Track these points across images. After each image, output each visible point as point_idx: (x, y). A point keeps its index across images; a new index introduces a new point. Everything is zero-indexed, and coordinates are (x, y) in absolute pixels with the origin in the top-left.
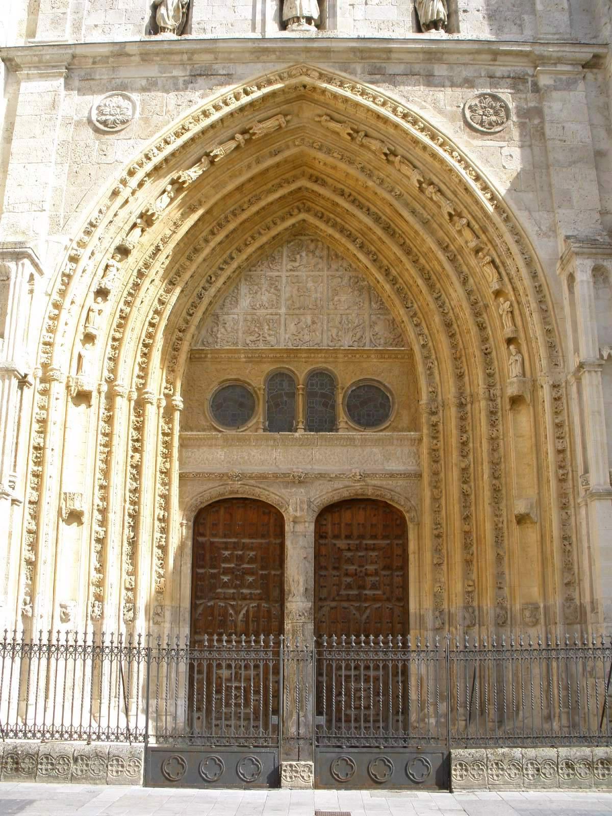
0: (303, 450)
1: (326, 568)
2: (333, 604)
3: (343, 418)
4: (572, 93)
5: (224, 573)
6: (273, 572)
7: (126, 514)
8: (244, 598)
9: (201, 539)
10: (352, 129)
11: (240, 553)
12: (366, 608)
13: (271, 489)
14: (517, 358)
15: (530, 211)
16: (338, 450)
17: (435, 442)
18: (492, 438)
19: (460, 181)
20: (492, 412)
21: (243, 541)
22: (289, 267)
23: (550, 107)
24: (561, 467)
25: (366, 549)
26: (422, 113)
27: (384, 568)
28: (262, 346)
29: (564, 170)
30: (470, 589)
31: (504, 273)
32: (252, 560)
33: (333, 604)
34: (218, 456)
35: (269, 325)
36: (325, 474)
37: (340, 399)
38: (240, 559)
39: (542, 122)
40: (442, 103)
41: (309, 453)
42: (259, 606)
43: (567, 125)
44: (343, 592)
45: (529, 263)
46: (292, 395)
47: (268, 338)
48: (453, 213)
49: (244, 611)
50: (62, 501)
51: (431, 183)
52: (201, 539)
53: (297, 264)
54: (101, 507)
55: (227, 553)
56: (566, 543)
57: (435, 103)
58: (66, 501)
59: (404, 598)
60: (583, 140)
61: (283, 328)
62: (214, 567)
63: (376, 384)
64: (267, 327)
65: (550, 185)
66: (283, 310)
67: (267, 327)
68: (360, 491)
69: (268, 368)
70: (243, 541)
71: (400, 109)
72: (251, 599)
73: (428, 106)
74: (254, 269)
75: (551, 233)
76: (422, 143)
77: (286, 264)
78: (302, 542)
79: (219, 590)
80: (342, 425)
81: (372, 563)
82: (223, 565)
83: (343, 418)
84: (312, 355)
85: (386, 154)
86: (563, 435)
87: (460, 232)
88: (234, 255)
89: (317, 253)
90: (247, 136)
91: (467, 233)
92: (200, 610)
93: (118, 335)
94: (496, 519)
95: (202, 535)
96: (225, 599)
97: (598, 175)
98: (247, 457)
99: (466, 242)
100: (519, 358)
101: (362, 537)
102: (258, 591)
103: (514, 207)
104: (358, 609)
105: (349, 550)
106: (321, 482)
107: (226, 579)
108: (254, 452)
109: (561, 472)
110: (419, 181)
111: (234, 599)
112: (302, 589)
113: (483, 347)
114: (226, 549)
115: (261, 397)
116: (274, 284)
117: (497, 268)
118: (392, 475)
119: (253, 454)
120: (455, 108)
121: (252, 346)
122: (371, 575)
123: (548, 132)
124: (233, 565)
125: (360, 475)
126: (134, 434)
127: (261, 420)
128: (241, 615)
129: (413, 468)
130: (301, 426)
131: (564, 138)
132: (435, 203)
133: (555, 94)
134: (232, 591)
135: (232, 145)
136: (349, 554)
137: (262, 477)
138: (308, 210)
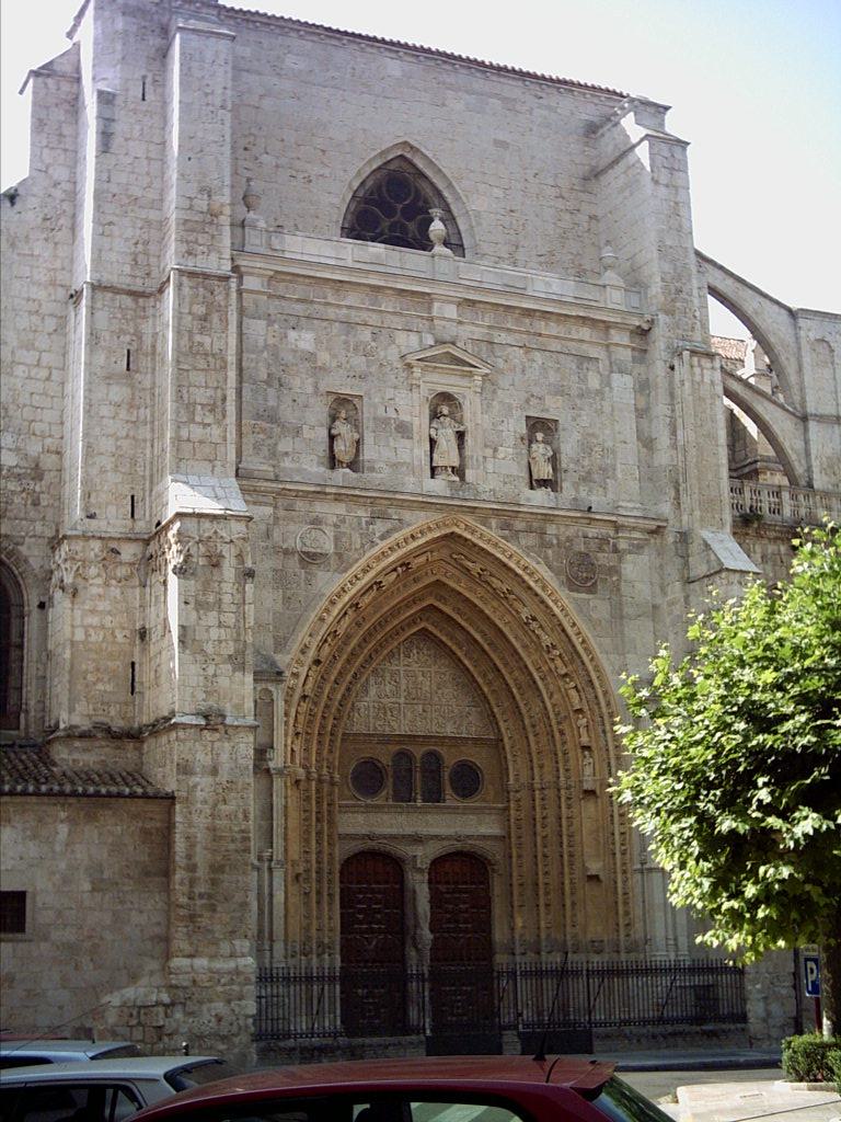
3: (448, 791)
26: (537, 566)
37: (446, 775)
44: (444, 926)
51: (534, 619)
71: (522, 562)
79: (356, 926)
83: (448, 791)
91: (558, 662)
100: (591, 760)
101: (456, 883)
107: (361, 916)
108: (385, 817)
117: (578, 691)
118: (484, 837)
136: (448, 896)
137: (393, 837)
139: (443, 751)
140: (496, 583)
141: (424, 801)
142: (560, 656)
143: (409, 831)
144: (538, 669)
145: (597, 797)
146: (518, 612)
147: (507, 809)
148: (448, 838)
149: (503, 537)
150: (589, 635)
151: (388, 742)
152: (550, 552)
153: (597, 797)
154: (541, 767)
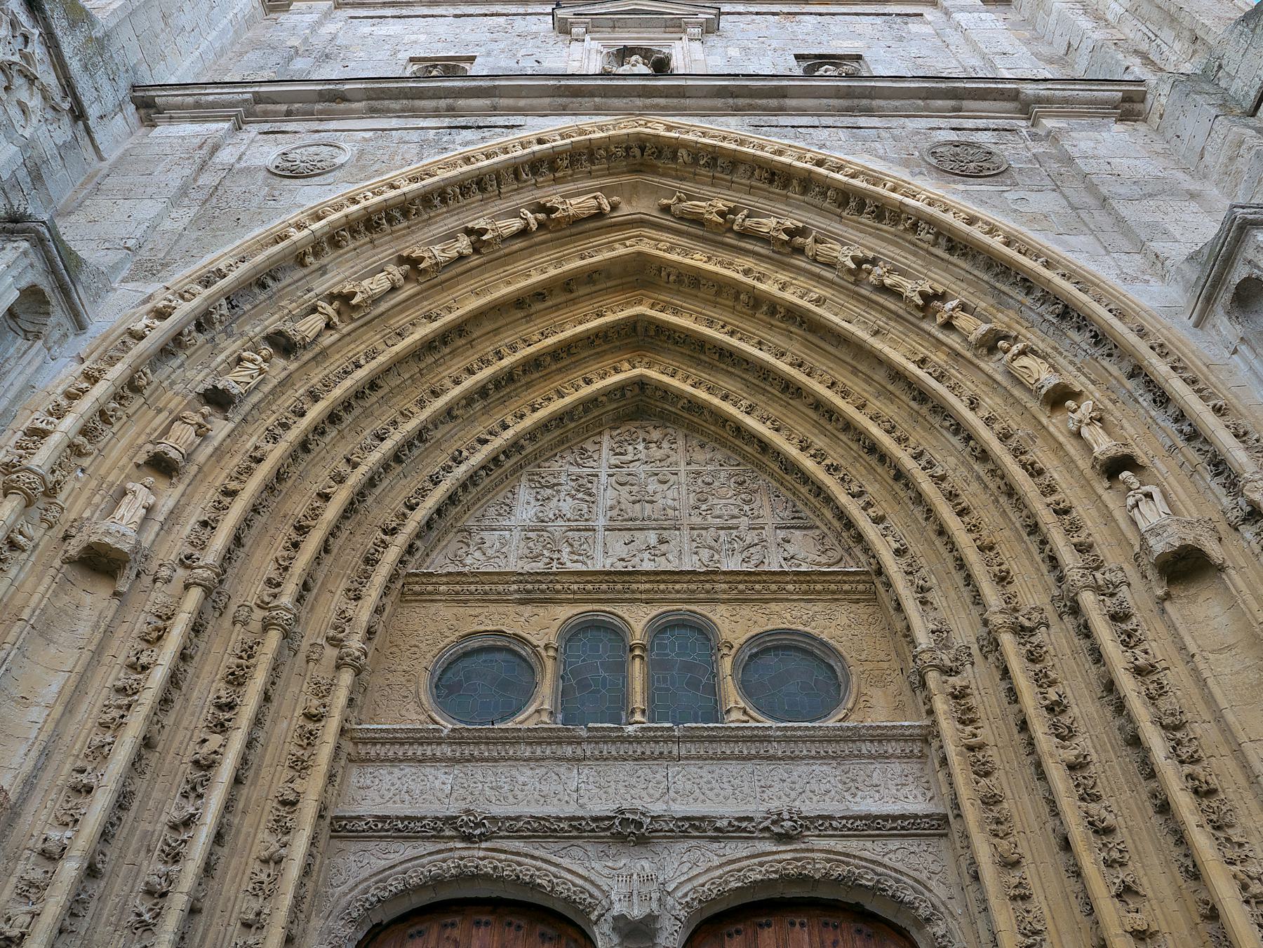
0: (644, 771)
13: (565, 862)
16: (733, 767)
17: (969, 729)
34: (437, 783)
35: (571, 545)
36: (702, 819)
41: (659, 776)
61: (600, 547)
64: (569, 549)
66: (601, 522)
67: (569, 549)
74: (547, 464)
90: (541, 216)
91: (963, 321)
98: (507, 787)
106: (693, 843)
115: (549, 664)
116: (585, 489)
119: (521, 779)
125: (791, 819)
126: (223, 693)
135: (516, 224)
140: (768, 225)
144: (922, 362)
145: (1221, 569)
146: (830, 265)
147: (929, 735)
153: (1221, 569)
154: (1003, 579)
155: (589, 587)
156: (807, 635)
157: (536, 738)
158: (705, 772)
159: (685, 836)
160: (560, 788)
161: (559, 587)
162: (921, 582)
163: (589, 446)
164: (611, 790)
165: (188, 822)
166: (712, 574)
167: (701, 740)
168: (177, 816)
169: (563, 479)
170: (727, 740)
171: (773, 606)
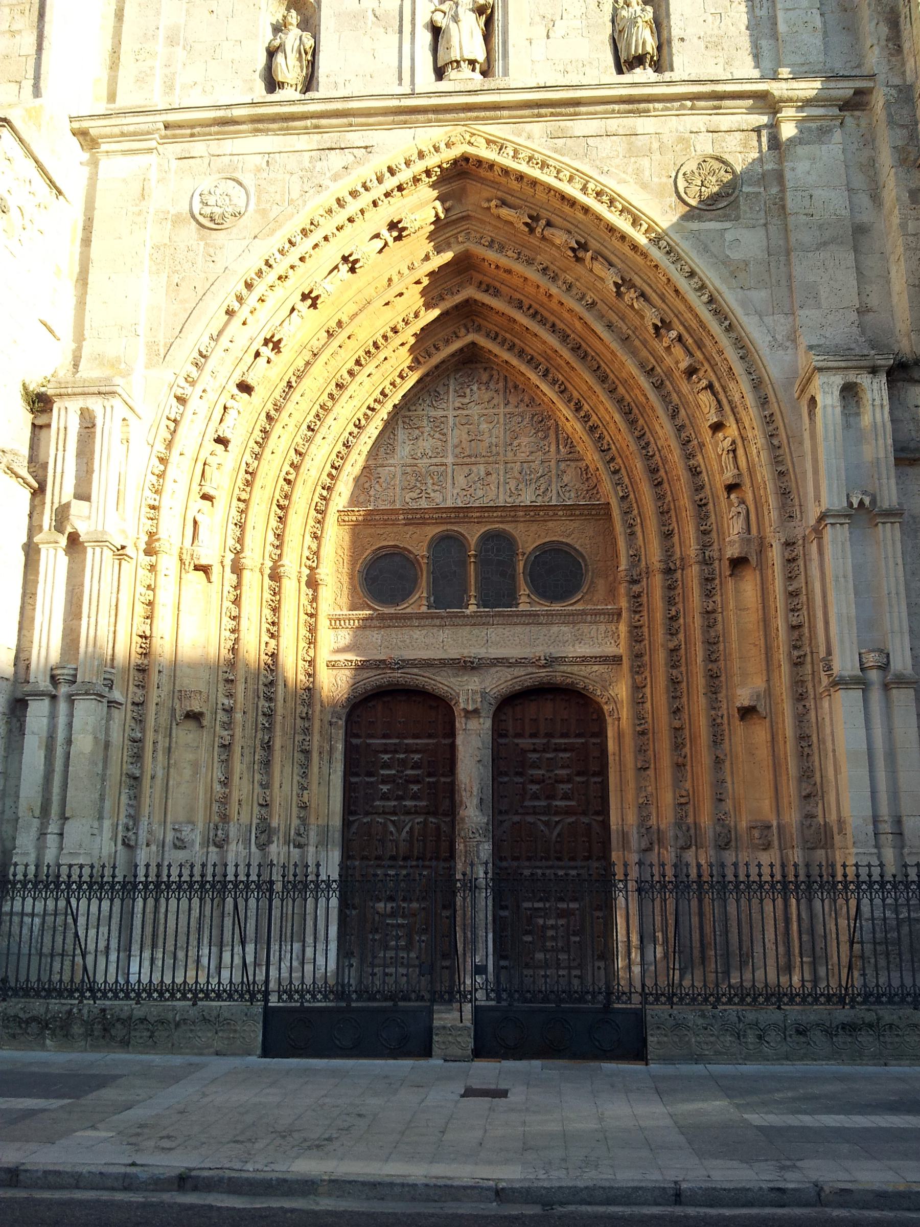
0: (476, 631)
1: (506, 774)
2: (516, 818)
3: (524, 590)
4: (824, 147)
5: (384, 782)
6: (443, 779)
7: (260, 713)
8: (408, 813)
9: (355, 741)
10: (530, 217)
11: (402, 756)
12: (557, 823)
13: (438, 678)
14: (739, 509)
15: (760, 316)
16: (519, 629)
17: (637, 617)
18: (708, 612)
19: (669, 280)
20: (707, 579)
21: (406, 741)
22: (457, 405)
23: (793, 169)
24: (795, 647)
25: (556, 750)
27: (579, 774)
28: (424, 504)
29: (810, 255)
30: (683, 800)
31: (724, 402)
32: (416, 766)
33: (516, 818)
34: (374, 639)
35: (433, 478)
36: (503, 659)
37: (521, 566)
38: (403, 763)
39: (783, 190)
40: (647, 173)
42: (425, 823)
43: (817, 193)
45: (757, 385)
46: (463, 564)
47: (432, 495)
48: (660, 324)
49: (407, 829)
50: (176, 701)
52: (355, 741)
53: (466, 400)
54: (227, 707)
55: (386, 757)
56: (804, 744)
57: (638, 172)
58: (180, 700)
59: (604, 810)
60: (838, 212)
61: (450, 481)
62: (370, 774)
63: (566, 549)
64: (431, 481)
65: (790, 277)
66: (450, 460)
67: (431, 481)
68: (545, 680)
69: (433, 531)
70: (406, 741)
71: (591, 186)
72: (416, 813)
73: (628, 178)
74: (414, 408)
75: (788, 344)
76: (620, 231)
77: (453, 400)
78: (476, 742)
79: (377, 803)
80: (523, 599)
81: (563, 767)
82: (382, 772)
83: (524, 590)
84: (486, 514)
85: (573, 250)
86: (799, 607)
87: (668, 349)
88: (387, 391)
89: (492, 386)
91: (678, 350)
92: (354, 829)
93: (244, 496)
94: (713, 712)
95: (357, 736)
96: (384, 813)
97: (856, 261)
98: (408, 641)
99: (677, 363)
101: (549, 735)
102: (424, 803)
103: (739, 311)
104: (546, 824)
105: (535, 751)
106: (498, 668)
107: (385, 788)
108: (417, 634)
109: (796, 653)
110: (616, 284)
111: (394, 813)
112: (475, 801)
113: (697, 498)
114: (386, 752)
115: (424, 567)
116: (438, 424)
117: (715, 394)
119: (415, 636)
120: (664, 180)
121: (414, 505)
122: (562, 782)
123: (789, 204)
124: (393, 772)
125: (545, 659)
126: (268, 617)
127: (425, 595)
128: (404, 834)
129: (611, 649)
130: (473, 601)
131: (810, 211)
132: (637, 312)
133: (801, 150)
134: (393, 803)
136: (534, 756)
137: (427, 664)
138: (479, 329)
139: (518, 531)
141: (484, 602)
142: (680, 338)
143: (453, 653)
148: (519, 663)
149: (556, 151)
150: (723, 288)
151: (423, 522)
152: (645, 162)
155: (444, 515)
156: (567, 544)
157: (421, 616)
158: (507, 631)
159: (495, 665)
160: (434, 641)
161: (427, 516)
162: (632, 521)
163: (441, 390)
164: (460, 642)
165: (272, 683)
166: (515, 508)
167: (503, 616)
168: (267, 681)
169: (425, 423)
170: (517, 616)
171: (550, 524)
